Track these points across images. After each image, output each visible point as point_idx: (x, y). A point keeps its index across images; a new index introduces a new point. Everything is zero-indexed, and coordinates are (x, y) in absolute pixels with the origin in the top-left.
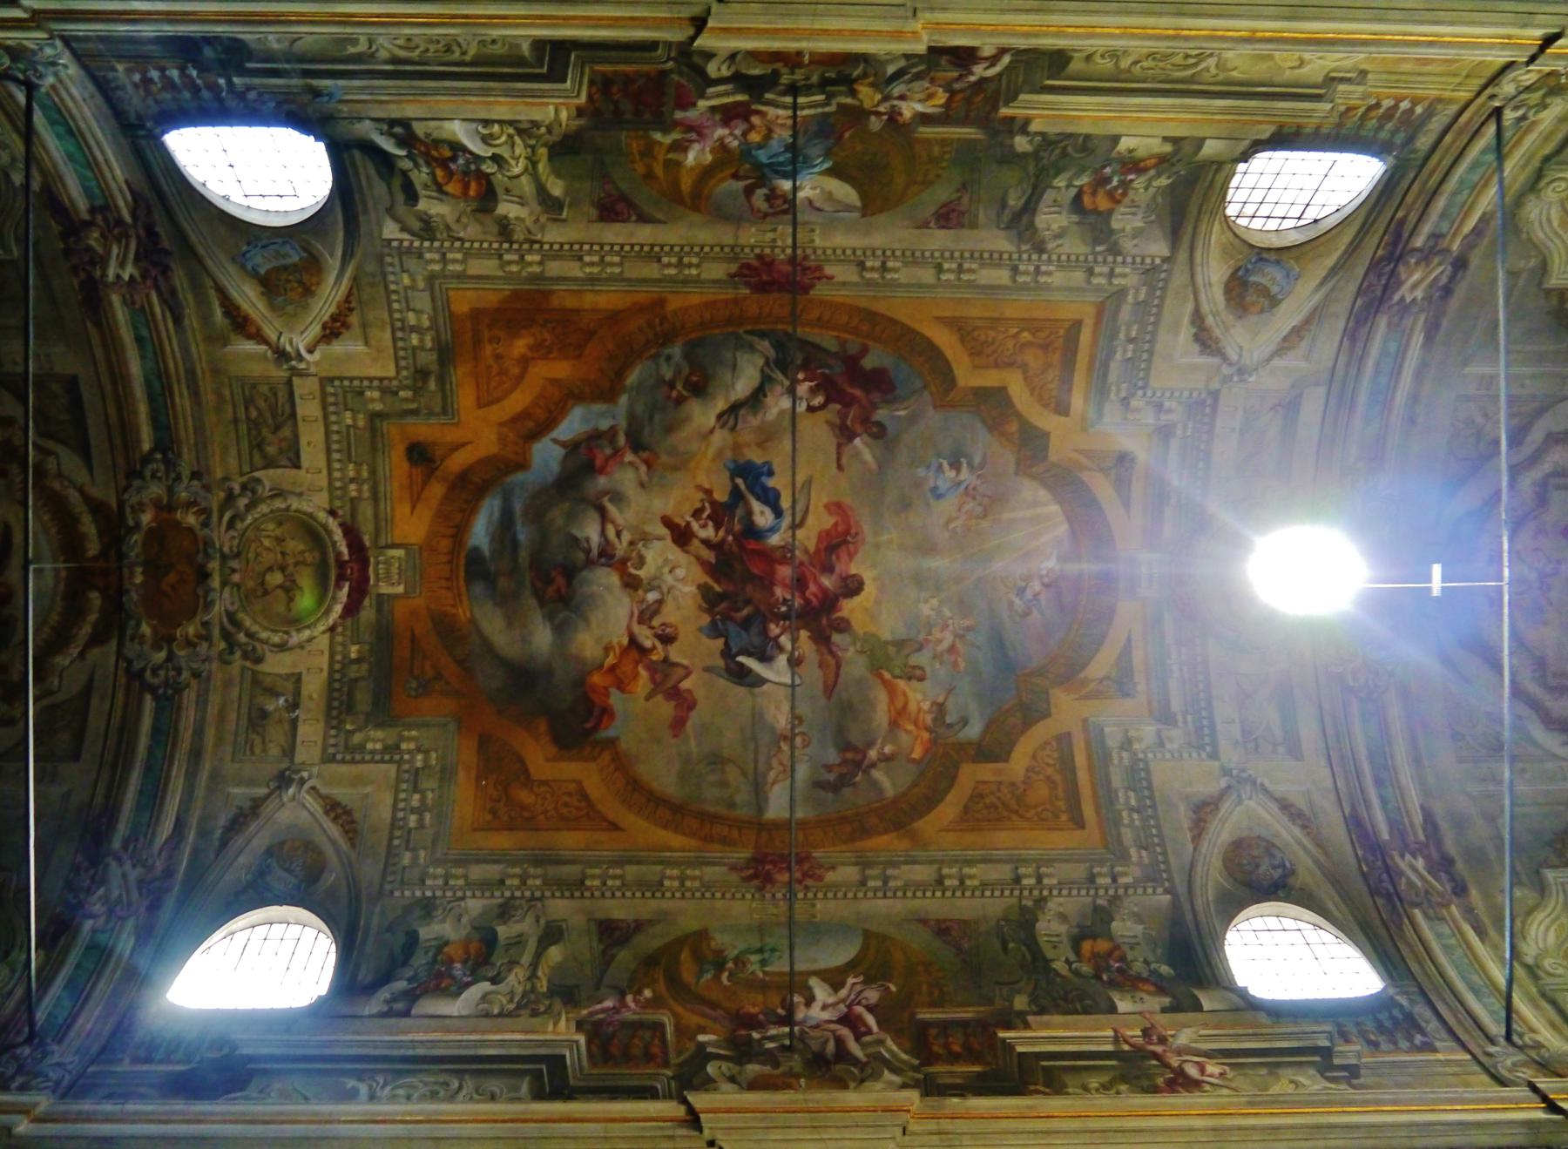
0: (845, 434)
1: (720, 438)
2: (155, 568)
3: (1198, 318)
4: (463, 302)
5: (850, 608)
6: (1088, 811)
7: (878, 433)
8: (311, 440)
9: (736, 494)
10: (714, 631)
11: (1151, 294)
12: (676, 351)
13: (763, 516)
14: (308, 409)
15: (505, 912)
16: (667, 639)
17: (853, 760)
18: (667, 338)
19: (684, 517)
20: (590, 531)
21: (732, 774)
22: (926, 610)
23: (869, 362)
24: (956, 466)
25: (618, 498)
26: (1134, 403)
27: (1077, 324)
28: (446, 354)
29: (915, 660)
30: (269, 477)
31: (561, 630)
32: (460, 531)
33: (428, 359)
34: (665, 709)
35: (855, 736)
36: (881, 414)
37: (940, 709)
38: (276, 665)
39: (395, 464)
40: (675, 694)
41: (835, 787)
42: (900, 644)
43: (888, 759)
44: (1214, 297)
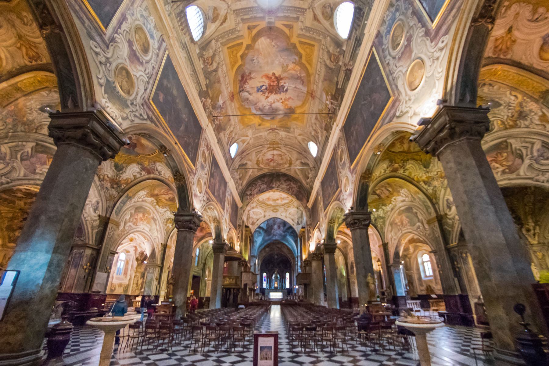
0: (251, 78)
1: (253, 95)
2: (273, 144)
3: (221, 24)
4: (242, 127)
5: (277, 75)
6: (312, 43)
7: (250, 73)
8: (259, 135)
9: (261, 91)
10: (280, 93)
11: (219, 38)
12: (243, 104)
13: (264, 88)
14: (256, 135)
15: (312, 127)
16: (281, 99)
17: (299, 78)
18: (242, 105)
19: (265, 97)
20: (267, 107)
21: (300, 95)
22: (277, 63)
23: (240, 78)
24: (253, 60)
25: (263, 105)
26: (239, 29)
27: (228, 48)
28: (248, 126)
29: (285, 65)
30: (263, 137)
31: (280, 110)
32: (269, 121)
33: (249, 127)
34: (290, 101)
35: (296, 77)
36: (247, 74)
37: (293, 63)
38: (284, 136)
39: (261, 127)
40: (289, 99)
41: (303, 82)
42: (283, 67)
43: (300, 73)
44: (218, 23)
